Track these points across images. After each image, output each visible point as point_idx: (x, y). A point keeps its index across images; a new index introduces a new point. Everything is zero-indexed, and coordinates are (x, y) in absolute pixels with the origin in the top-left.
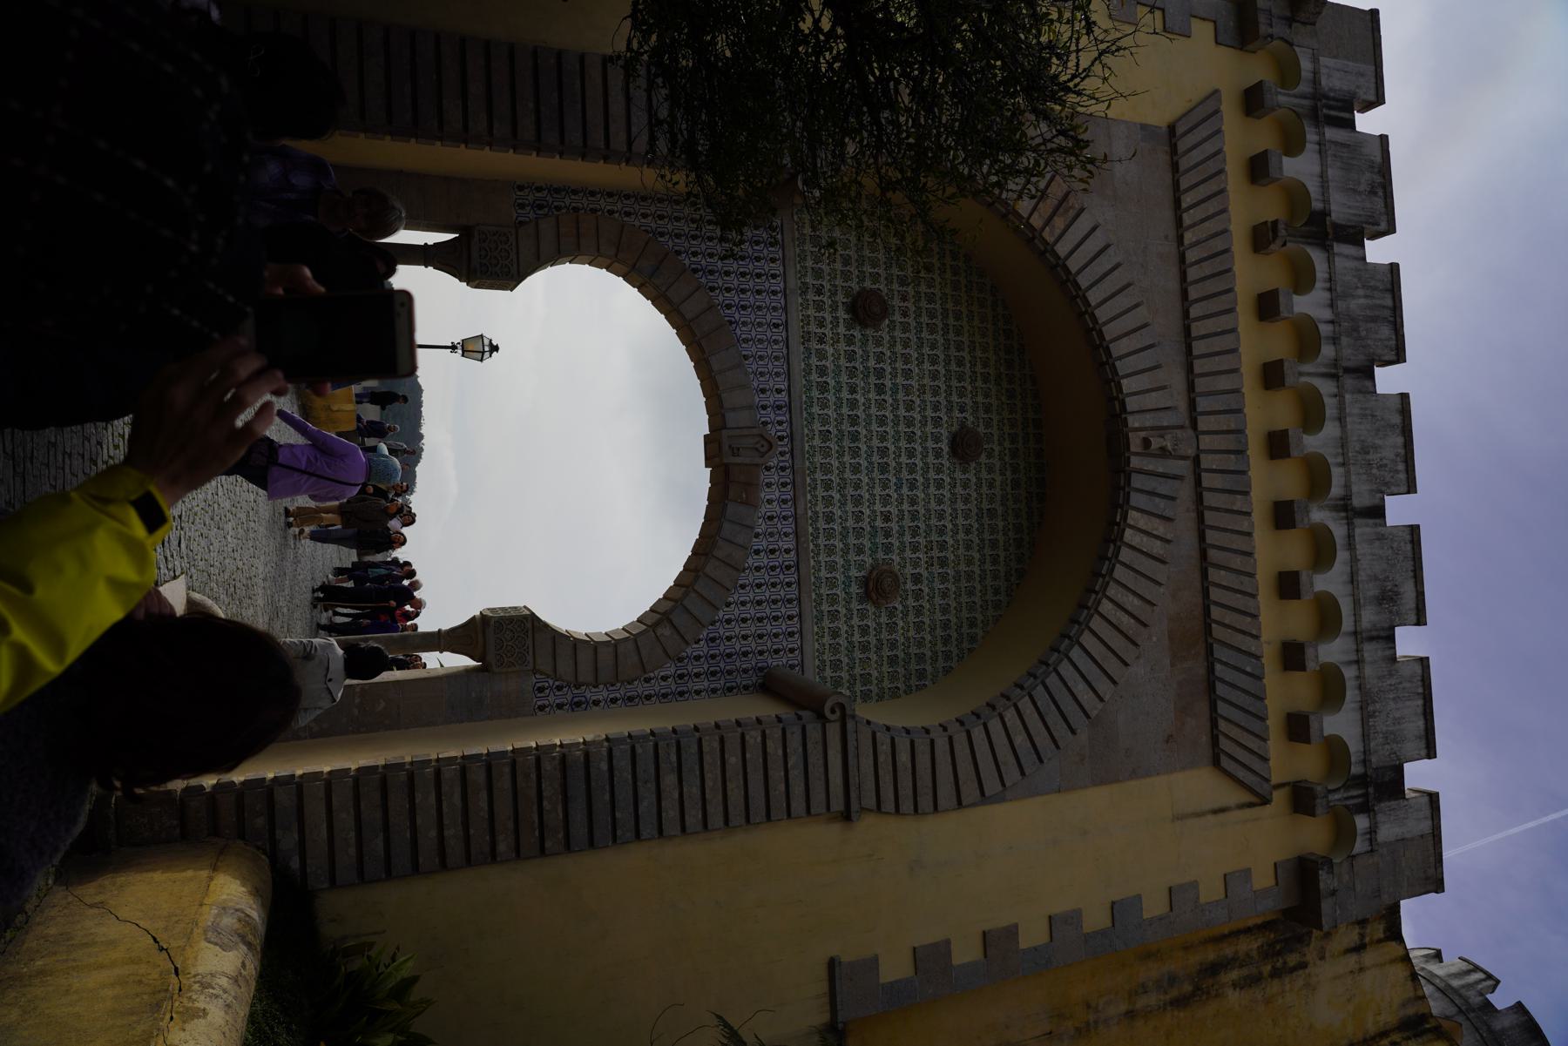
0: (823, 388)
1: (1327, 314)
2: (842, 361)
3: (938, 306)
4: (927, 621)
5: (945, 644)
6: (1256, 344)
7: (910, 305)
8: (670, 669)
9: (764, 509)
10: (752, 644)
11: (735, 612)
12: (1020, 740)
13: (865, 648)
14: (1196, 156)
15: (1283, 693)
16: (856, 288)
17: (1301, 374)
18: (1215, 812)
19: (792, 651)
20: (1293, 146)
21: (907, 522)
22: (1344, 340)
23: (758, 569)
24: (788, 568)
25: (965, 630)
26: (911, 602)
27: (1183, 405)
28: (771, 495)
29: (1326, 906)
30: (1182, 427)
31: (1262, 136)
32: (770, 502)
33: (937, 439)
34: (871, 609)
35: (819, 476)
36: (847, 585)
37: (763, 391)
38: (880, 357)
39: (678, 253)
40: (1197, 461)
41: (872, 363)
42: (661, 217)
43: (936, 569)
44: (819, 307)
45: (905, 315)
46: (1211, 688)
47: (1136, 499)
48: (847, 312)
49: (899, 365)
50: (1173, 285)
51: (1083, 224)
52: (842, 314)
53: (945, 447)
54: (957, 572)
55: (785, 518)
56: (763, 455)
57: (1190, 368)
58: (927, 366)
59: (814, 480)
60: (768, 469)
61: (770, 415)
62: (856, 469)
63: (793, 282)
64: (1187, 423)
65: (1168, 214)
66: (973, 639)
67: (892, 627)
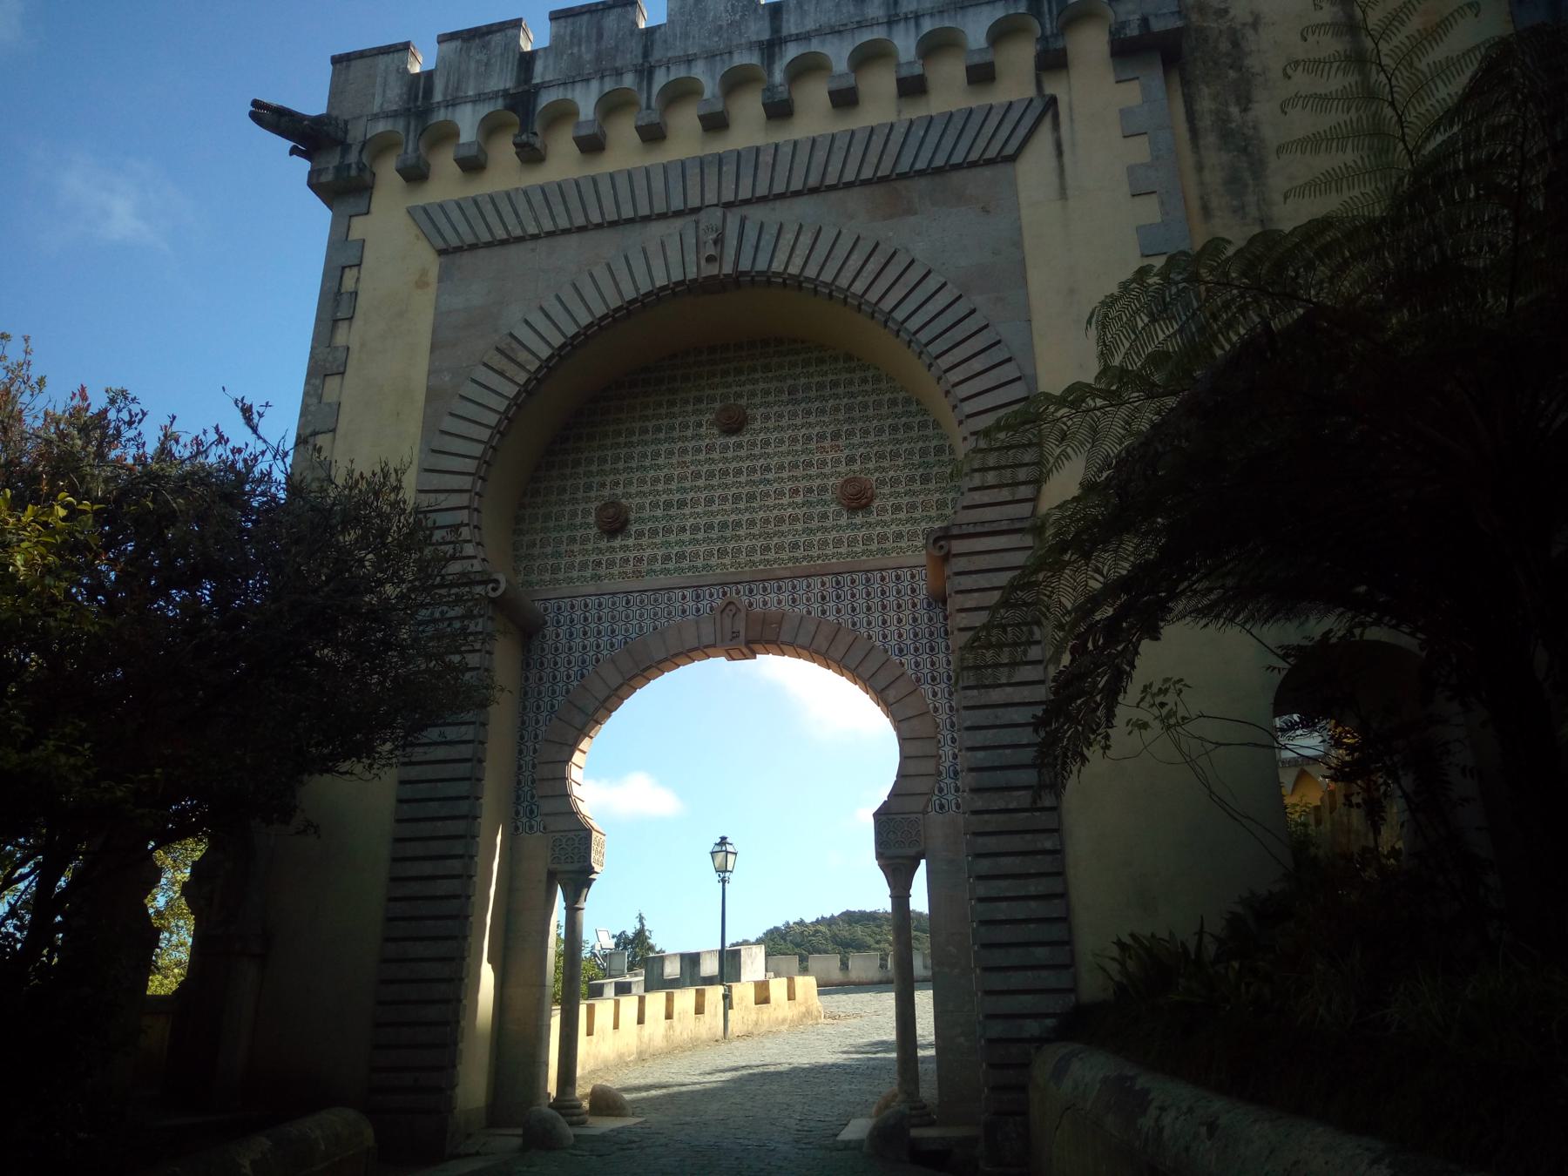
0: (681, 557)
1: (595, 84)
4: (890, 447)
5: (912, 428)
6: (624, 151)
7: (609, 480)
8: (927, 689)
10: (906, 614)
12: (977, 365)
13: (912, 507)
14: (463, 228)
15: (949, 92)
16: (595, 530)
17: (649, 107)
19: (913, 576)
20: (449, 133)
22: (618, 64)
24: (838, 583)
25: (899, 410)
27: (678, 223)
28: (772, 601)
29: (1157, 26)
30: (697, 222)
31: (445, 164)
32: (779, 602)
33: (726, 448)
34: (876, 503)
36: (854, 527)
37: (684, 611)
38: (654, 505)
39: (568, 691)
40: (728, 205)
41: (659, 513)
42: (538, 707)
44: (611, 564)
46: (939, 171)
47: (761, 265)
49: (660, 487)
50: (574, 239)
51: (524, 333)
52: (617, 543)
54: (846, 421)
55: (794, 587)
56: (738, 610)
57: (646, 219)
58: (661, 461)
59: (761, 562)
60: (751, 604)
62: (752, 523)
63: (591, 589)
64: (694, 217)
65: (513, 250)
66: (907, 401)
67: (895, 482)
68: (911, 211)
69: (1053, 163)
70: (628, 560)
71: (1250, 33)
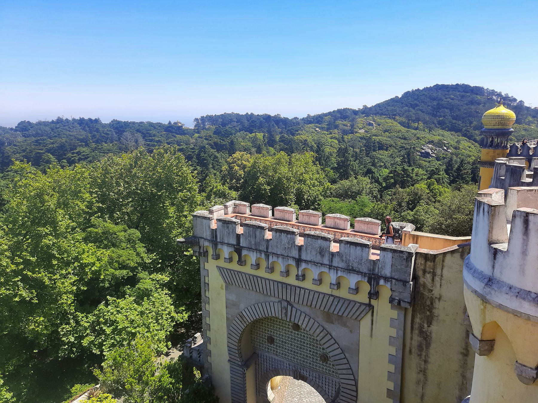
11: (327, 390)
18: (372, 324)
68: (332, 323)
69: (370, 325)
71: (437, 301)
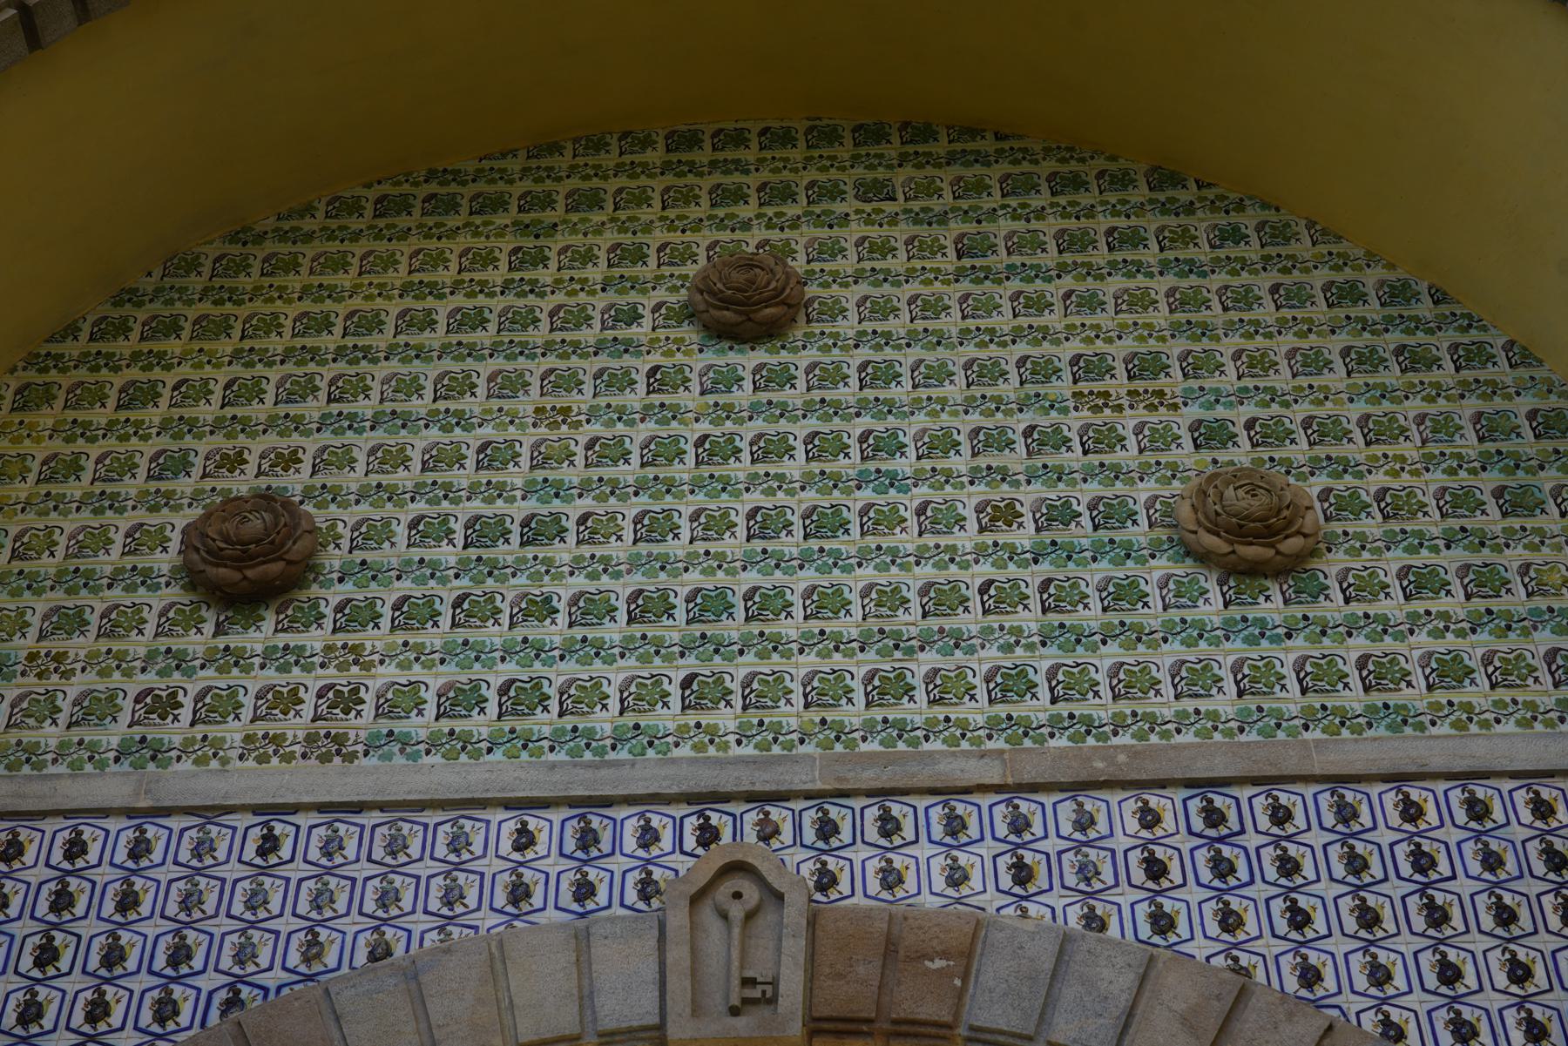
0: (521, 698)
2: (432, 638)
3: (274, 374)
9: (987, 892)
11: (1416, 1004)
16: (174, 594)
21: (1017, 459)
23: (1229, 921)
24: (1214, 817)
26: (1299, 452)
32: (957, 877)
34: (1333, 564)
35: (853, 714)
37: (519, 893)
41: (447, 554)
43: (1173, 382)
44: (216, 707)
45: (290, 460)
48: (255, 621)
49: (462, 477)
52: (258, 637)
53: (748, 360)
55: (1019, 825)
58: (470, 405)
60: (826, 881)
61: (617, 872)
62: (825, 603)
63: (115, 787)
66: (1397, 293)
67: (1392, 506)
70: (294, 698)
